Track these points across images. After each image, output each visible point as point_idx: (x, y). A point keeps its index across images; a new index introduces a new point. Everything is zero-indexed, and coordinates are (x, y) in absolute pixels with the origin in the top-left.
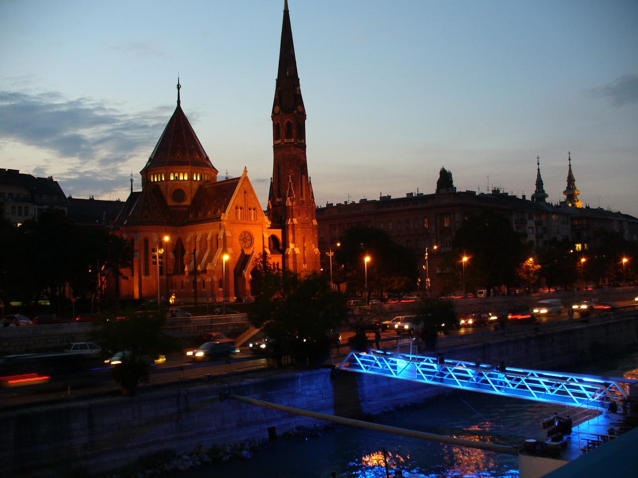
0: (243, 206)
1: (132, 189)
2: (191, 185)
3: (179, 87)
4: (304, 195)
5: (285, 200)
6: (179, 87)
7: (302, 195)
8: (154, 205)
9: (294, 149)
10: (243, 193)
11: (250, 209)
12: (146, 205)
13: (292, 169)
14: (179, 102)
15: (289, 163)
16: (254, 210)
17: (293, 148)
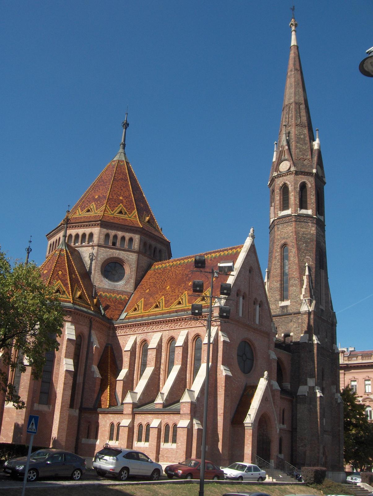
0: (247, 293)
3: (126, 125)
6: (126, 125)
8: (73, 276)
9: (312, 226)
12: (60, 273)
13: (310, 256)
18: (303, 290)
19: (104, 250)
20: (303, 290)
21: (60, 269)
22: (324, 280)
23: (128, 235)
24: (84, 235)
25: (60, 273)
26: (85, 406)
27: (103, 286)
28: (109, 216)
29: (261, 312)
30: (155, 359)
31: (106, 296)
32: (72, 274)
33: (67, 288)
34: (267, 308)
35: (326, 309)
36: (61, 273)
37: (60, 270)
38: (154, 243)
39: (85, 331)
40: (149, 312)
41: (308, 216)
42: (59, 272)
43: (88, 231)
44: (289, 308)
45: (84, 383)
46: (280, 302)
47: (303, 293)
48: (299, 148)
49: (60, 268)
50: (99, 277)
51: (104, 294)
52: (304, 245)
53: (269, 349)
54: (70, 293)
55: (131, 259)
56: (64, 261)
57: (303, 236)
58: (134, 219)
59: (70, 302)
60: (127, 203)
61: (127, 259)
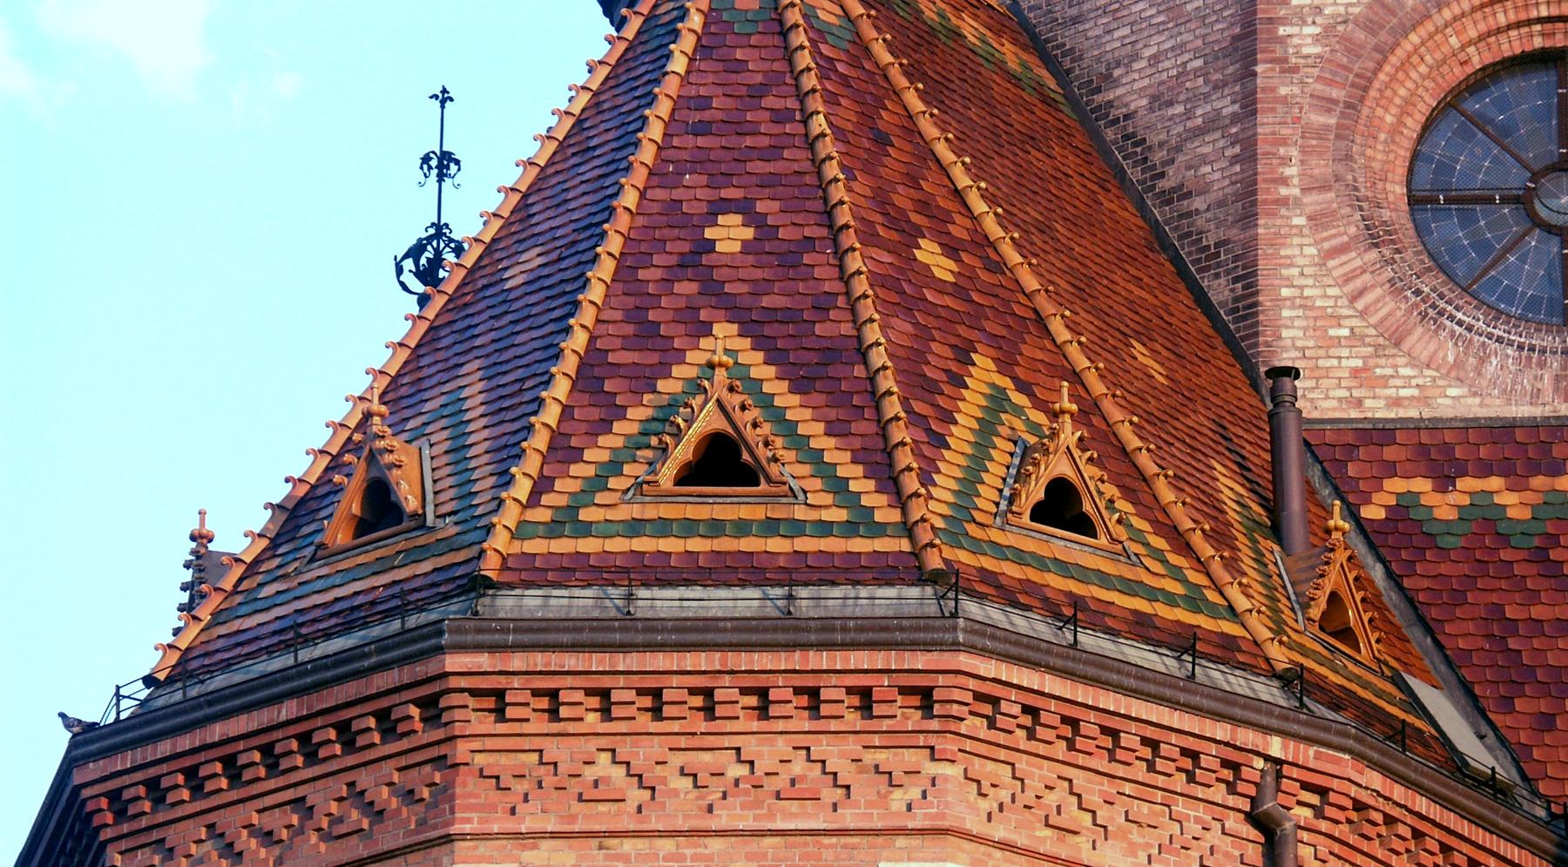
12: (730, 234)
21: (724, 193)
25: (730, 234)
27: (1424, 400)
31: (1484, 518)
32: (912, 235)
36: (749, 233)
37: (725, 206)
42: (709, 233)
49: (719, 179)
50: (1348, 279)
51: (1445, 506)
54: (904, 458)
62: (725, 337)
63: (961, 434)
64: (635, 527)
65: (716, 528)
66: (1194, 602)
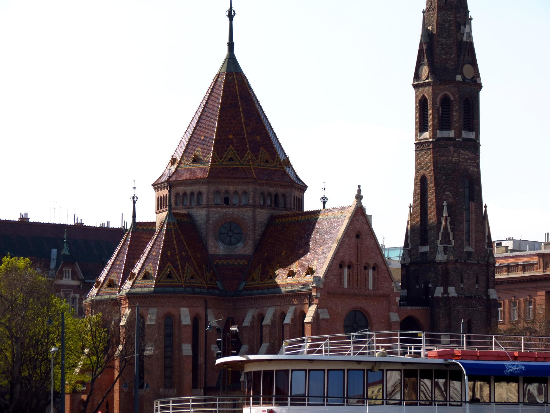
0: (354, 260)
1: (134, 216)
2: (254, 216)
3: (231, 15)
4: (473, 241)
5: (434, 249)
6: (231, 15)
7: (468, 240)
8: (183, 253)
9: (454, 152)
10: (354, 240)
11: (366, 268)
12: (169, 253)
14: (231, 45)
15: (444, 177)
16: (374, 269)
17: (452, 149)
18: (440, 234)
19: (215, 211)
20: (440, 234)
22: (473, 215)
23: (240, 188)
24: (192, 194)
25: (169, 253)
26: (208, 385)
28: (217, 168)
29: (376, 274)
30: (268, 335)
33: (178, 271)
34: (384, 268)
35: (476, 251)
38: (273, 190)
39: (201, 311)
40: (264, 283)
41: (449, 139)
43: (196, 189)
44: (428, 255)
45: (205, 363)
46: (420, 247)
47: (440, 238)
48: (442, 44)
51: (220, 263)
52: (444, 177)
53: (389, 312)
55: (247, 216)
56: (172, 237)
57: (442, 167)
58: (247, 165)
59: (181, 286)
60: (238, 143)
61: (242, 218)
62: (169, 264)
63: (185, 272)
64: (164, 282)
65: (169, 282)
66: (201, 283)
